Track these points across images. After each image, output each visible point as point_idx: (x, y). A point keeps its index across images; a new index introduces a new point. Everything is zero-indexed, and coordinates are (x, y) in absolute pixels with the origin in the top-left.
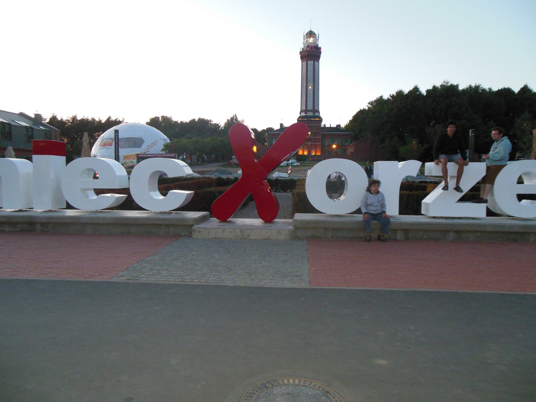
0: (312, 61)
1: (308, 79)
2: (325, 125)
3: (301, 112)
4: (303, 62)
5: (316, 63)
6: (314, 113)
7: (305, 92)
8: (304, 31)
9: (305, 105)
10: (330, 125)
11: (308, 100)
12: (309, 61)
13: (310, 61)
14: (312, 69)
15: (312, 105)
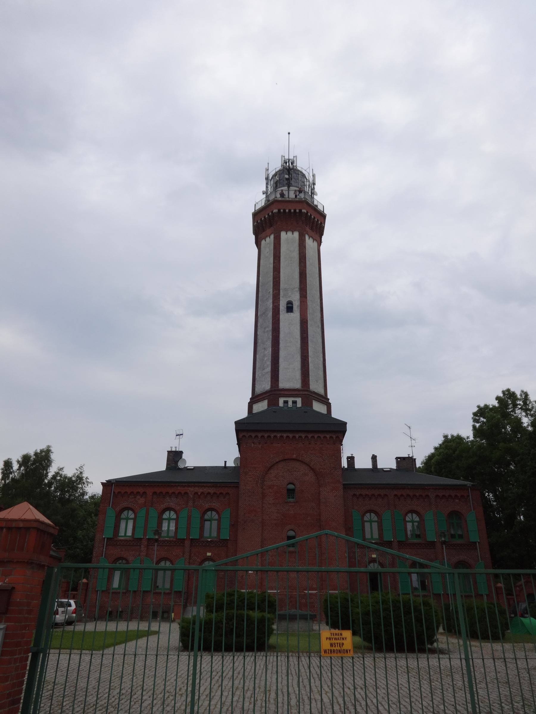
0: (296, 234)
1: (282, 286)
2: (351, 460)
3: (255, 399)
4: (263, 242)
5: (310, 243)
6: (307, 403)
7: (270, 328)
8: (268, 164)
9: (270, 374)
10: (374, 458)
11: (282, 354)
12: (283, 234)
13: (290, 233)
14: (296, 255)
15: (298, 375)
